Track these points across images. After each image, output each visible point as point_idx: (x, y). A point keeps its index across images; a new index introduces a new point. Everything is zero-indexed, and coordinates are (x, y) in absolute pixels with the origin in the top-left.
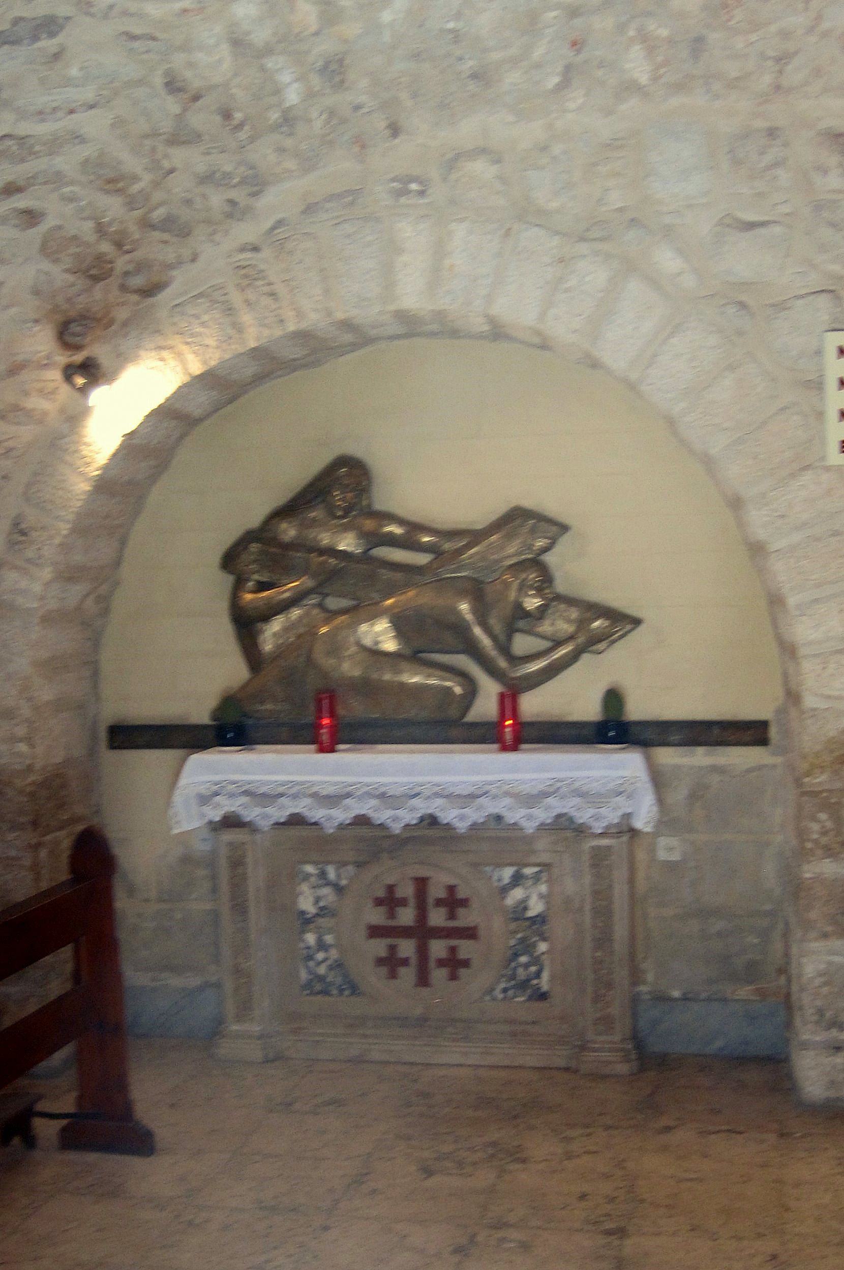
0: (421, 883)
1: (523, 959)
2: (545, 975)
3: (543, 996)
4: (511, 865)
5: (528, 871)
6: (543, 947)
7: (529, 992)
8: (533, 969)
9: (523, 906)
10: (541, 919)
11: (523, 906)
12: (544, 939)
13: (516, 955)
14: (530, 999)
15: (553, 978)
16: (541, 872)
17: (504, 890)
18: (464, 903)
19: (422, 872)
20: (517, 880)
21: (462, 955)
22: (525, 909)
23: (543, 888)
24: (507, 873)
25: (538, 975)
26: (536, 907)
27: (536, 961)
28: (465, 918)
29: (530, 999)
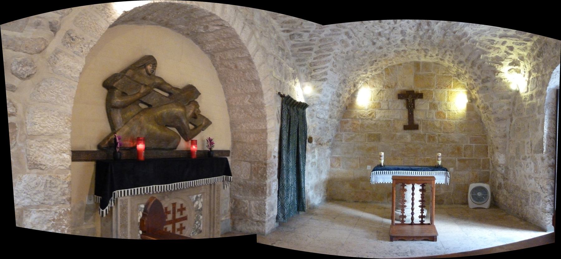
0: (174, 205)
1: (197, 222)
2: (201, 226)
3: (201, 232)
4: (195, 194)
5: (199, 195)
6: (201, 217)
7: (198, 232)
8: (199, 224)
9: (198, 206)
10: (201, 209)
11: (198, 206)
12: (201, 215)
13: (196, 221)
14: (198, 233)
15: (203, 226)
16: (201, 195)
17: (194, 203)
18: (184, 209)
19: (174, 201)
20: (197, 198)
21: (183, 226)
22: (198, 207)
23: (202, 200)
24: (195, 196)
25: (200, 226)
26: (200, 206)
27: (200, 221)
28: (185, 213)
29: (198, 233)
